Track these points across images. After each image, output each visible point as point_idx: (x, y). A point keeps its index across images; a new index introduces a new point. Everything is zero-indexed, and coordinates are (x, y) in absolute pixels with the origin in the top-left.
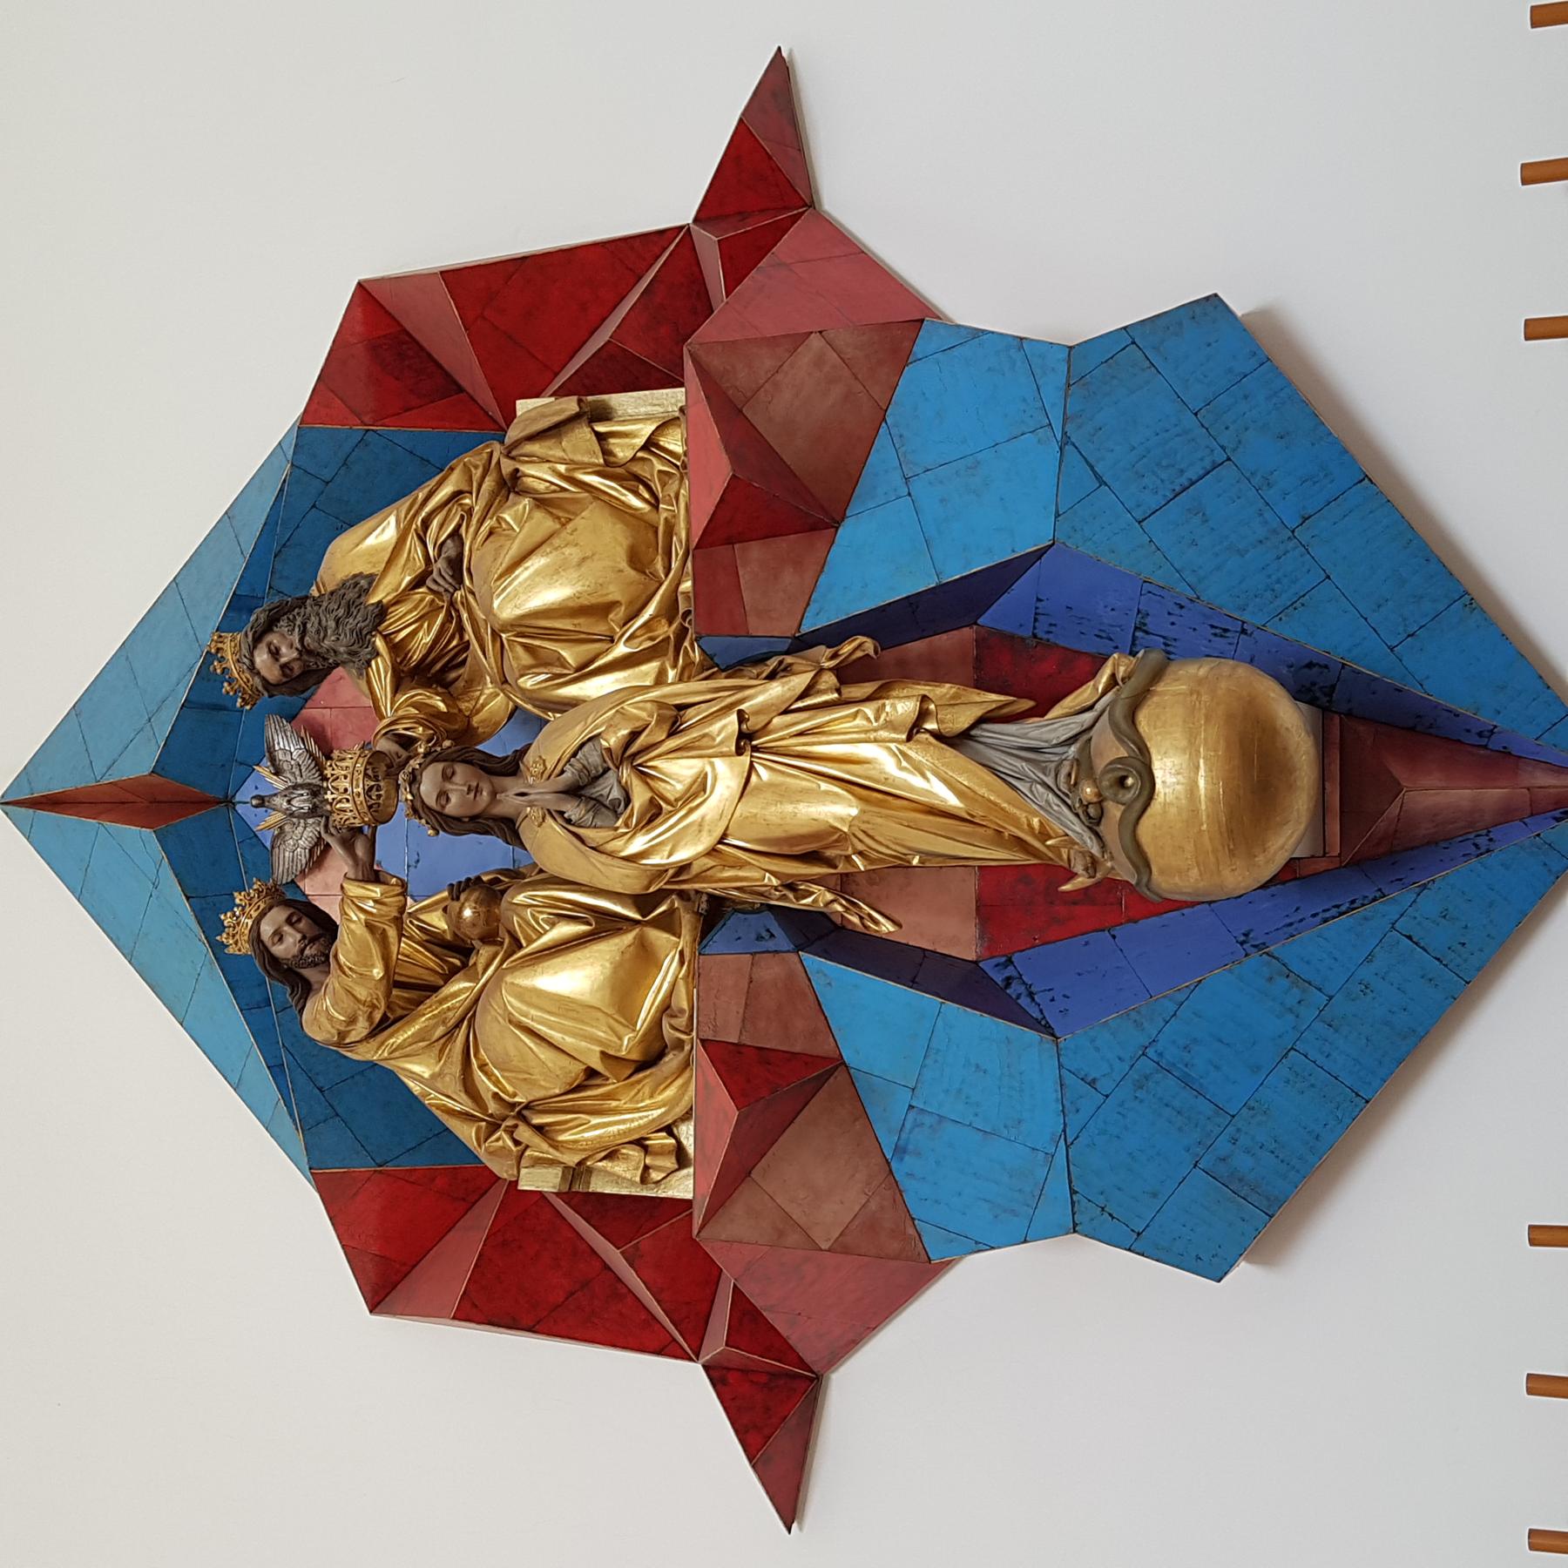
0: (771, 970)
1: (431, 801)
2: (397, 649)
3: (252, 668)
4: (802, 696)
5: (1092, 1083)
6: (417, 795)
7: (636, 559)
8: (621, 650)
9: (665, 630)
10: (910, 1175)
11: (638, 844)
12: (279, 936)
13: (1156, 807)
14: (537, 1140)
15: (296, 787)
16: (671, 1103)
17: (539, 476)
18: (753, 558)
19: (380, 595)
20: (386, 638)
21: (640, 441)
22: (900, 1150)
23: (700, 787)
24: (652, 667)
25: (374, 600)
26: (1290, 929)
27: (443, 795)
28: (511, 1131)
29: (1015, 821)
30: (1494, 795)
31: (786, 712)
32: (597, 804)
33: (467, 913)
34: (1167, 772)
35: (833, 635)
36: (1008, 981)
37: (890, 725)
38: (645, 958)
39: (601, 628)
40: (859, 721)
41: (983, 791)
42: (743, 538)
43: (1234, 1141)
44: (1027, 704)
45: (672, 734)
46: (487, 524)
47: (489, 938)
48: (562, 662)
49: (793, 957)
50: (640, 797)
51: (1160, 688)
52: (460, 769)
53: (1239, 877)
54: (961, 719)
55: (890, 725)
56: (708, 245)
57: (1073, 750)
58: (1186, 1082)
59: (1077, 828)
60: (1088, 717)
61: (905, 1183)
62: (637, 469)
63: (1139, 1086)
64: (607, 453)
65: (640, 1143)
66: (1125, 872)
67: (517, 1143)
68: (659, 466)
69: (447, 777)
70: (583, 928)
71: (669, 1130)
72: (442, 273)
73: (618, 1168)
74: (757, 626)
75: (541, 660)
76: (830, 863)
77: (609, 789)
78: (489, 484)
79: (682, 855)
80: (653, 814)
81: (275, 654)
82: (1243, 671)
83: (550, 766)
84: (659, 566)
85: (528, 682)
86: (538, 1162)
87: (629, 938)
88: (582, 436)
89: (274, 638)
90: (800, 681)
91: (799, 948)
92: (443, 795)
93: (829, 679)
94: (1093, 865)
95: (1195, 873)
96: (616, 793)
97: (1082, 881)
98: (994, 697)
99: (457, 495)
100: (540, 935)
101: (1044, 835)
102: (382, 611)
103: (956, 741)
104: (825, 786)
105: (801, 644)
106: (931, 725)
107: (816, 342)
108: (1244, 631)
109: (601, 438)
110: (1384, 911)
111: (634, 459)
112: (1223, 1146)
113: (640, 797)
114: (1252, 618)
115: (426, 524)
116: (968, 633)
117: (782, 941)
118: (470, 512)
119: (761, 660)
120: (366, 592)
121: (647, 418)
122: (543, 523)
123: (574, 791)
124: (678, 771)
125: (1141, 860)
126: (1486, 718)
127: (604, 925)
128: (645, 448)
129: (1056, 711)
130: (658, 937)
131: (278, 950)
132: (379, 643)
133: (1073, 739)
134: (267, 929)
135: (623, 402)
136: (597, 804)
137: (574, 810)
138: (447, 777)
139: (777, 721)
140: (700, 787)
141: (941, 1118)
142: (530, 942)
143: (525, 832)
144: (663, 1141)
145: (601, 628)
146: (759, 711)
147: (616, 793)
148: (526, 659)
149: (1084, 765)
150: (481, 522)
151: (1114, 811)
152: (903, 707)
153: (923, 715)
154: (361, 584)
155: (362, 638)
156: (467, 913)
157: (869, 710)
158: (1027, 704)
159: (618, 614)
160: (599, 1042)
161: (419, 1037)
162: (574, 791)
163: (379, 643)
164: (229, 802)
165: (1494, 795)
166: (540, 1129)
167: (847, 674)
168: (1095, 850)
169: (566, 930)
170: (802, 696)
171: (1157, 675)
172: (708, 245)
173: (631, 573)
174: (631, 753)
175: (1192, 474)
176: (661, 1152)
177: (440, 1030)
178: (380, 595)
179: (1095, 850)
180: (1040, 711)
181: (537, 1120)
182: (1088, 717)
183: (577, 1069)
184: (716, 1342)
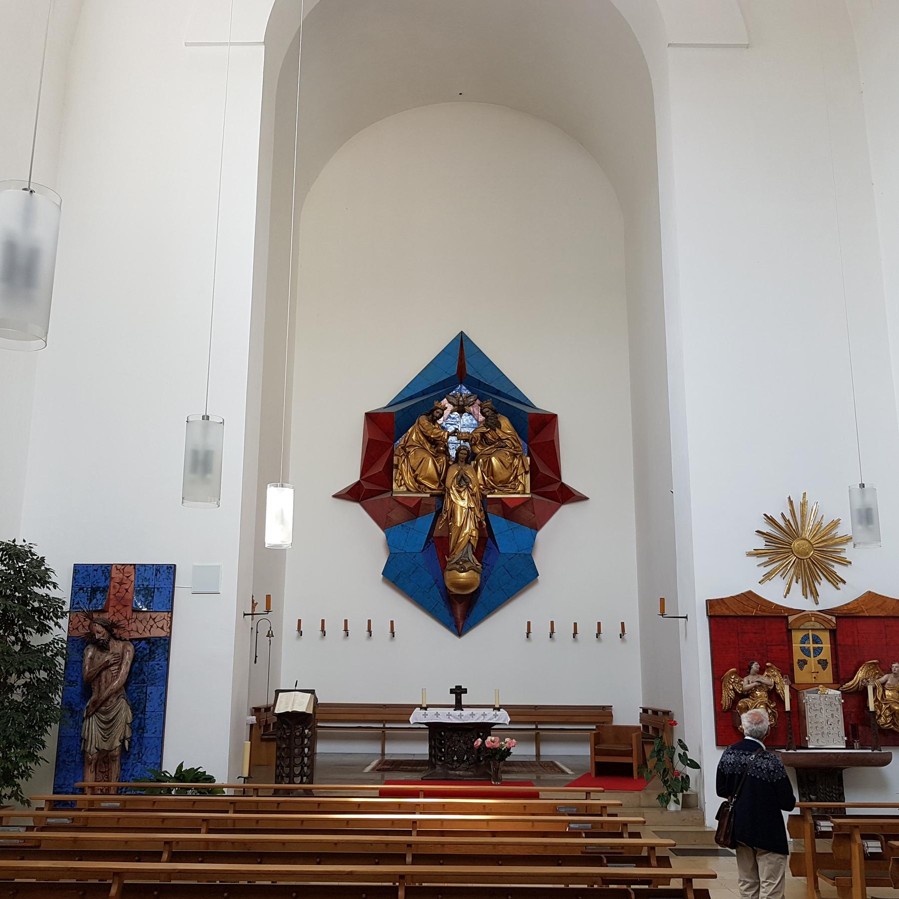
0: (433, 507)
1: (461, 452)
2: (488, 432)
3: (484, 408)
4: (477, 517)
5: (414, 557)
6: (462, 450)
7: (500, 482)
8: (486, 478)
9: (489, 486)
10: (398, 527)
11: (454, 488)
12: (438, 412)
13: (458, 573)
14: (402, 460)
15: (464, 402)
16: (409, 485)
17: (516, 461)
18: (499, 506)
19: (498, 431)
20: (489, 431)
21: (521, 481)
22: (403, 526)
23: (463, 499)
24: (483, 483)
25: (497, 429)
26: (438, 587)
27: (462, 454)
28: (404, 454)
29: (457, 550)
30: (459, 617)
31: (474, 514)
32: (460, 481)
33: (442, 448)
34: (464, 574)
35: (487, 520)
36: (430, 542)
37: (471, 532)
38: (434, 482)
39: (490, 474)
40: (472, 527)
41: (461, 546)
42: (502, 505)
43: (405, 578)
44: (474, 551)
45: (471, 495)
46: (508, 453)
47: (437, 451)
48: (483, 469)
49: (435, 510)
50: (461, 489)
51: (476, 573)
52: (466, 456)
53: (447, 584)
54: (472, 542)
55: (471, 532)
56: (555, 487)
57: (467, 559)
58: (414, 571)
59: (455, 560)
60: (472, 561)
61: (397, 527)
62: (517, 480)
63: (414, 564)
64: (519, 475)
65: (402, 479)
66: (448, 567)
67: (402, 456)
68: (517, 484)
69: (465, 454)
70: (439, 471)
71: (404, 484)
72: (553, 441)
73: (398, 475)
74: (489, 506)
75: (485, 463)
76: (450, 519)
77: (463, 483)
78: (515, 452)
79: (452, 495)
80: (459, 492)
81: (488, 411)
82: (478, 585)
83: (466, 472)
84: (500, 485)
85: (481, 460)
86: (398, 460)
87: (438, 480)
88: (523, 471)
89: (490, 411)
90: (479, 516)
91: (436, 511)
92: (462, 454)
93: (479, 520)
94: (450, 562)
95: (448, 578)
96: (462, 485)
97: (447, 559)
98: (476, 545)
99: (514, 445)
100: (438, 463)
101: (454, 554)
102: (495, 430)
103: (469, 541)
104: (462, 520)
105: (485, 513)
106: (471, 538)
107: (534, 515)
108: (485, 581)
109: (522, 474)
110: (441, 601)
111: (518, 480)
112: (404, 576)
113: (461, 489)
114: (487, 583)
115: (509, 440)
116: (487, 536)
117: (437, 509)
118: (511, 448)
119: (483, 506)
120: (498, 427)
121: (525, 482)
122: (508, 465)
123: (462, 477)
124: (465, 495)
125: (450, 570)
126: (471, 616)
127: (439, 475)
128: (520, 481)
129: (473, 556)
130: (437, 485)
131: (435, 412)
132: (489, 429)
133: (469, 559)
134: (438, 410)
135: (529, 476)
136: (460, 481)
137: (459, 477)
138: (465, 454)
139: (473, 512)
140: (463, 499)
141: (408, 533)
142: (436, 460)
143: (455, 465)
144: (403, 482)
145: (490, 474)
146: (475, 510)
147: (462, 485)
148: (485, 460)
149: (465, 562)
150: (508, 451)
151: (458, 567)
152: (474, 533)
153: (473, 537)
154: (499, 427)
155: (489, 426)
156: (442, 448)
157: (474, 528)
158: (474, 551)
159: (492, 478)
160: (420, 473)
161: (420, 438)
162: (462, 477)
163: (489, 429)
164: (461, 383)
165: (459, 617)
166: (404, 460)
167: (480, 523)
168: (452, 563)
169: (439, 468)
170: (477, 517)
171: (478, 572)
172: (555, 487)
173: (498, 481)
174: (468, 487)
175: (510, 573)
176: (401, 483)
177: (421, 443)
178: (498, 431)
179: (452, 563)
180: (473, 553)
181: (406, 460)
182: (472, 561)
183: (415, 469)
184: (367, 486)
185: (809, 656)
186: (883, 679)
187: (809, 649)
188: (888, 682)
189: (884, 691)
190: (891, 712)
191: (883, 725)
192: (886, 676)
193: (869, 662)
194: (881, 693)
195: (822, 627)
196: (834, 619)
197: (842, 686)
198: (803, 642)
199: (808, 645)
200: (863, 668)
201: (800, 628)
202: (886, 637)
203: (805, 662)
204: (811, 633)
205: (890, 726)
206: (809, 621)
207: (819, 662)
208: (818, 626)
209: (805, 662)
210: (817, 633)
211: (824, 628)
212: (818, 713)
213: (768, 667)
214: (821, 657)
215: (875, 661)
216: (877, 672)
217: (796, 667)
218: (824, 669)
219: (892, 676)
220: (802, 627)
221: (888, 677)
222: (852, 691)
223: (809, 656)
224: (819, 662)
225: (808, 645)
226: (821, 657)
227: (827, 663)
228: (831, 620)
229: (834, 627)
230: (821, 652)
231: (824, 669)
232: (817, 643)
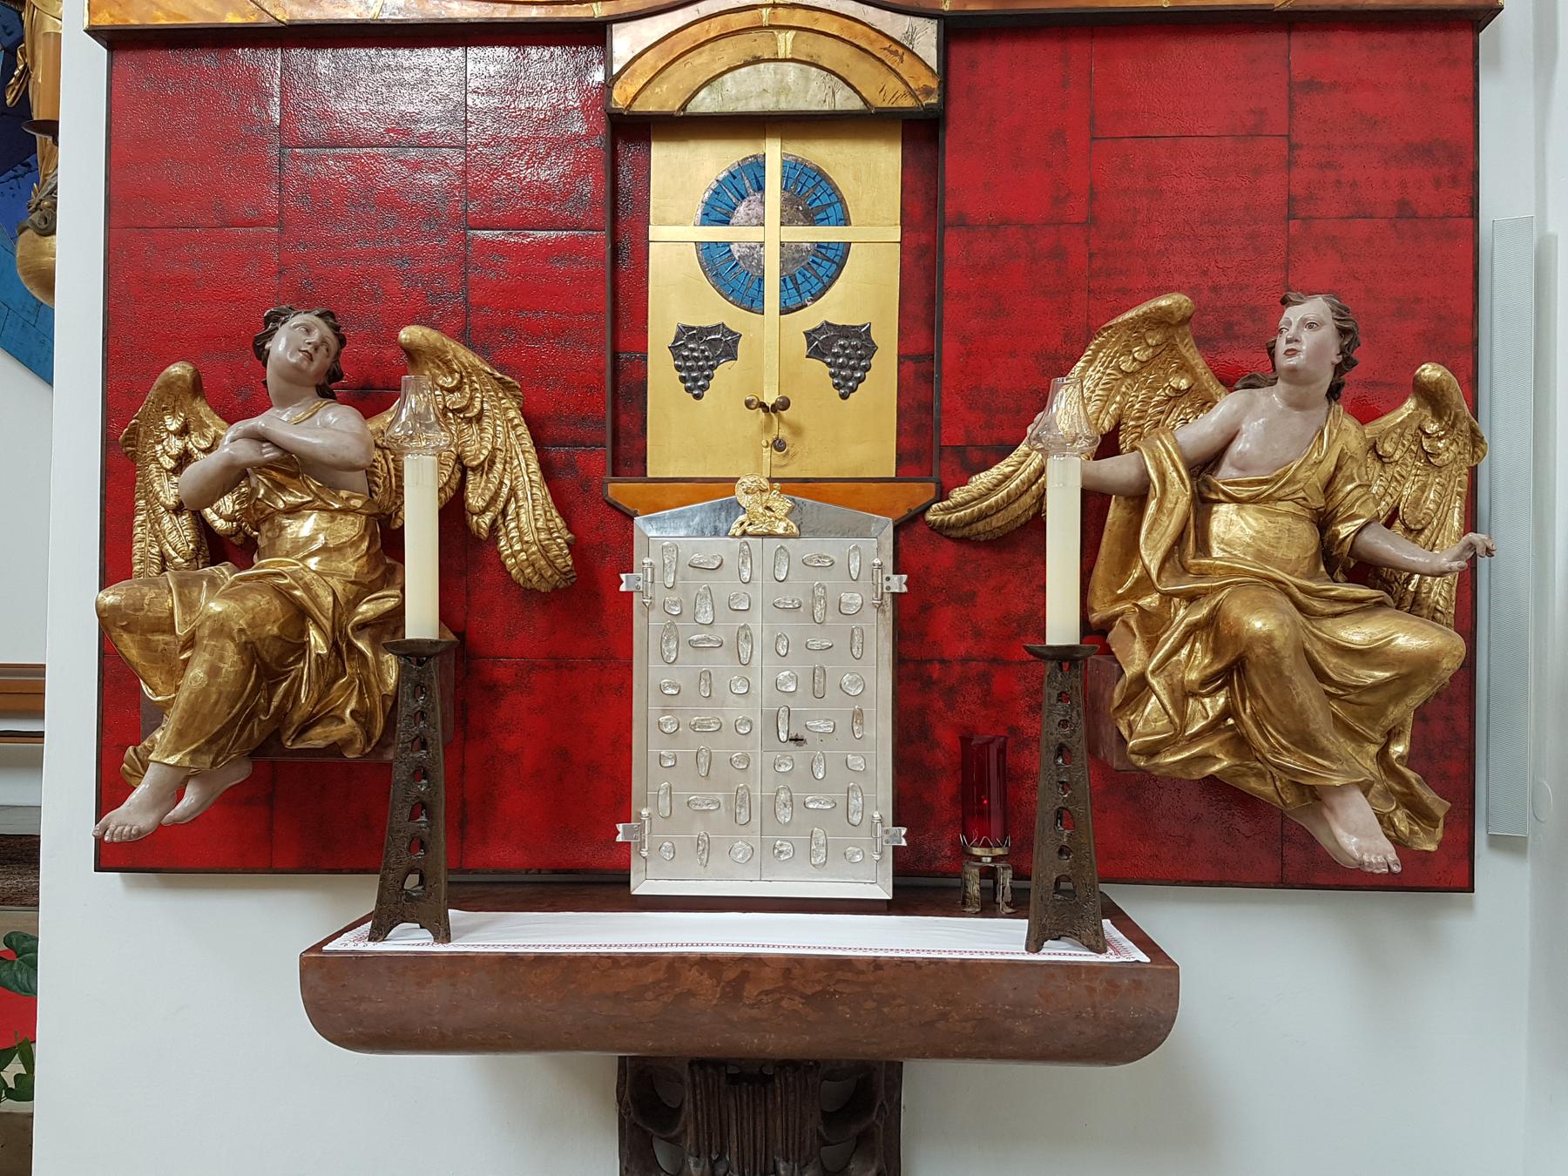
185: (753, 303)
186: (1200, 430)
187: (755, 252)
188: (1239, 446)
189: (1203, 504)
190: (1216, 652)
191: (1152, 750)
192: (1228, 405)
193: (1128, 316)
194: (1171, 526)
195: (845, 101)
196: (926, 39)
197: (942, 495)
198: (718, 211)
199: (753, 234)
200: (1090, 362)
201: (693, 108)
202: (1290, 164)
203: (720, 344)
204: (773, 152)
205: (1205, 758)
206: (757, 60)
207: (822, 343)
208: (814, 94)
209: (720, 344)
210: (821, 153)
211: (857, 104)
212: (720, 663)
213: (412, 354)
214: (834, 307)
215: (1164, 302)
216: (1184, 384)
217: (661, 372)
218: (846, 386)
219: (1271, 398)
220: (706, 103)
221: (1249, 405)
222: (997, 521)
223: (753, 303)
224: (822, 343)
225: (753, 234)
226: (834, 307)
227: (870, 349)
228: (903, 48)
229: (928, 92)
230: (833, 279)
231: (846, 386)
232: (811, 219)
